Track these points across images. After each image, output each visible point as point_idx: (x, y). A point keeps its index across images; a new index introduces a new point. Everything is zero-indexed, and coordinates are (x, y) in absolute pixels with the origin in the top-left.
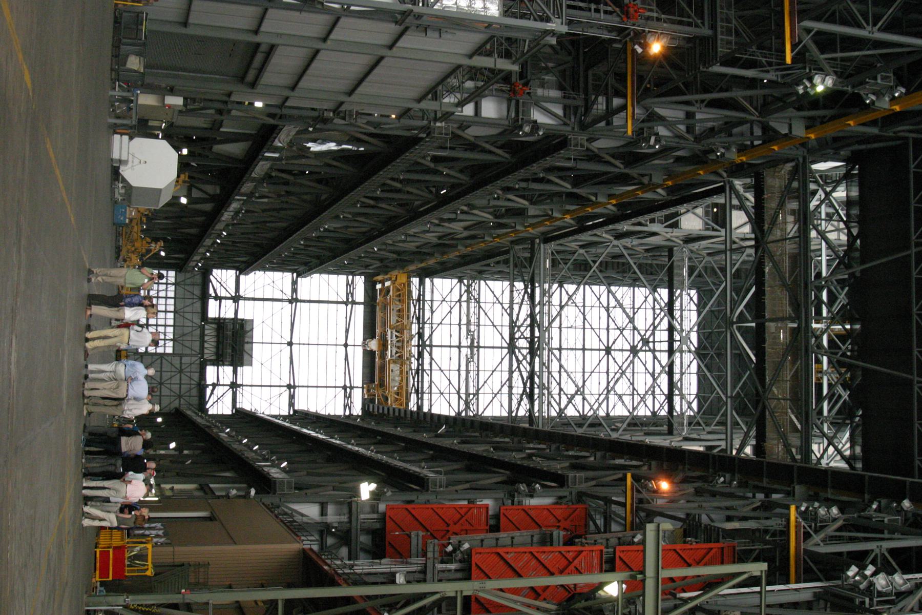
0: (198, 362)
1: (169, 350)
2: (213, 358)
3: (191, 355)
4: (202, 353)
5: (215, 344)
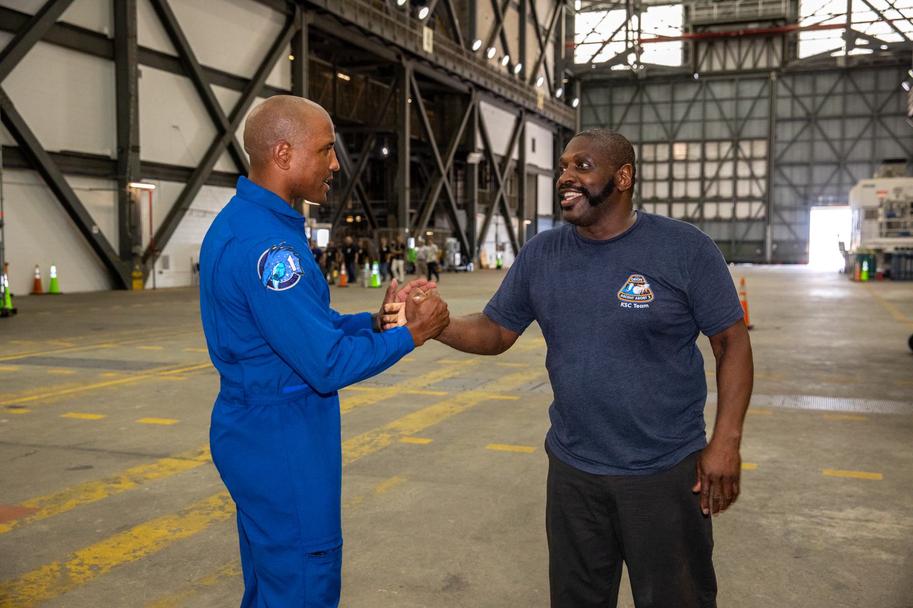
1: (761, 149)
3: (772, 98)
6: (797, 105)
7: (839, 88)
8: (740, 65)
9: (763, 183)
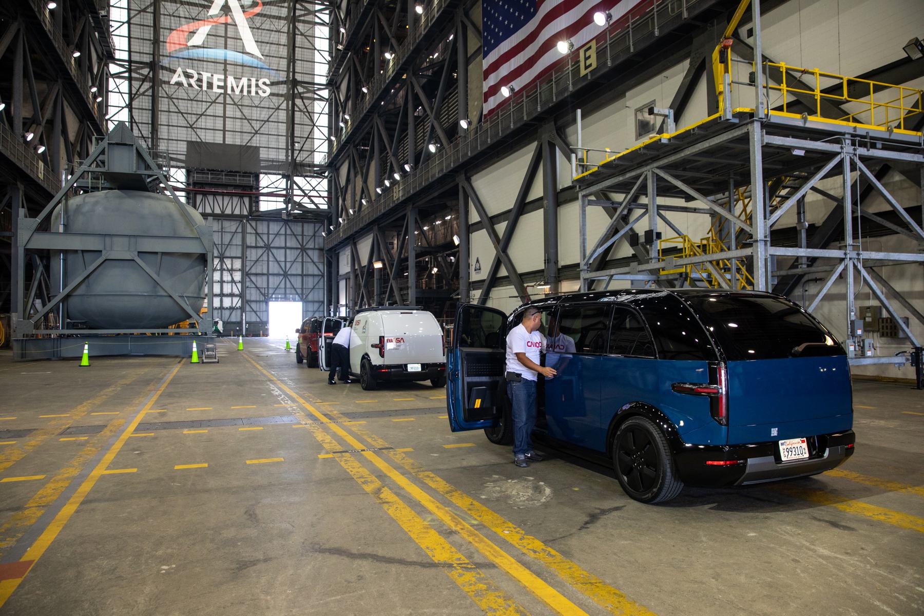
0: (253, 224)
1: (238, 264)
2: (246, 200)
3: (244, 232)
4: (240, 217)
5: (226, 199)
6: (258, 238)
7: (283, 231)
8: (223, 212)
9: (239, 285)
